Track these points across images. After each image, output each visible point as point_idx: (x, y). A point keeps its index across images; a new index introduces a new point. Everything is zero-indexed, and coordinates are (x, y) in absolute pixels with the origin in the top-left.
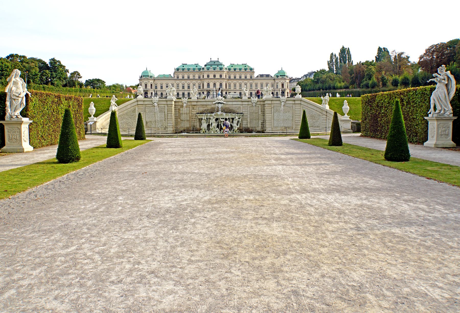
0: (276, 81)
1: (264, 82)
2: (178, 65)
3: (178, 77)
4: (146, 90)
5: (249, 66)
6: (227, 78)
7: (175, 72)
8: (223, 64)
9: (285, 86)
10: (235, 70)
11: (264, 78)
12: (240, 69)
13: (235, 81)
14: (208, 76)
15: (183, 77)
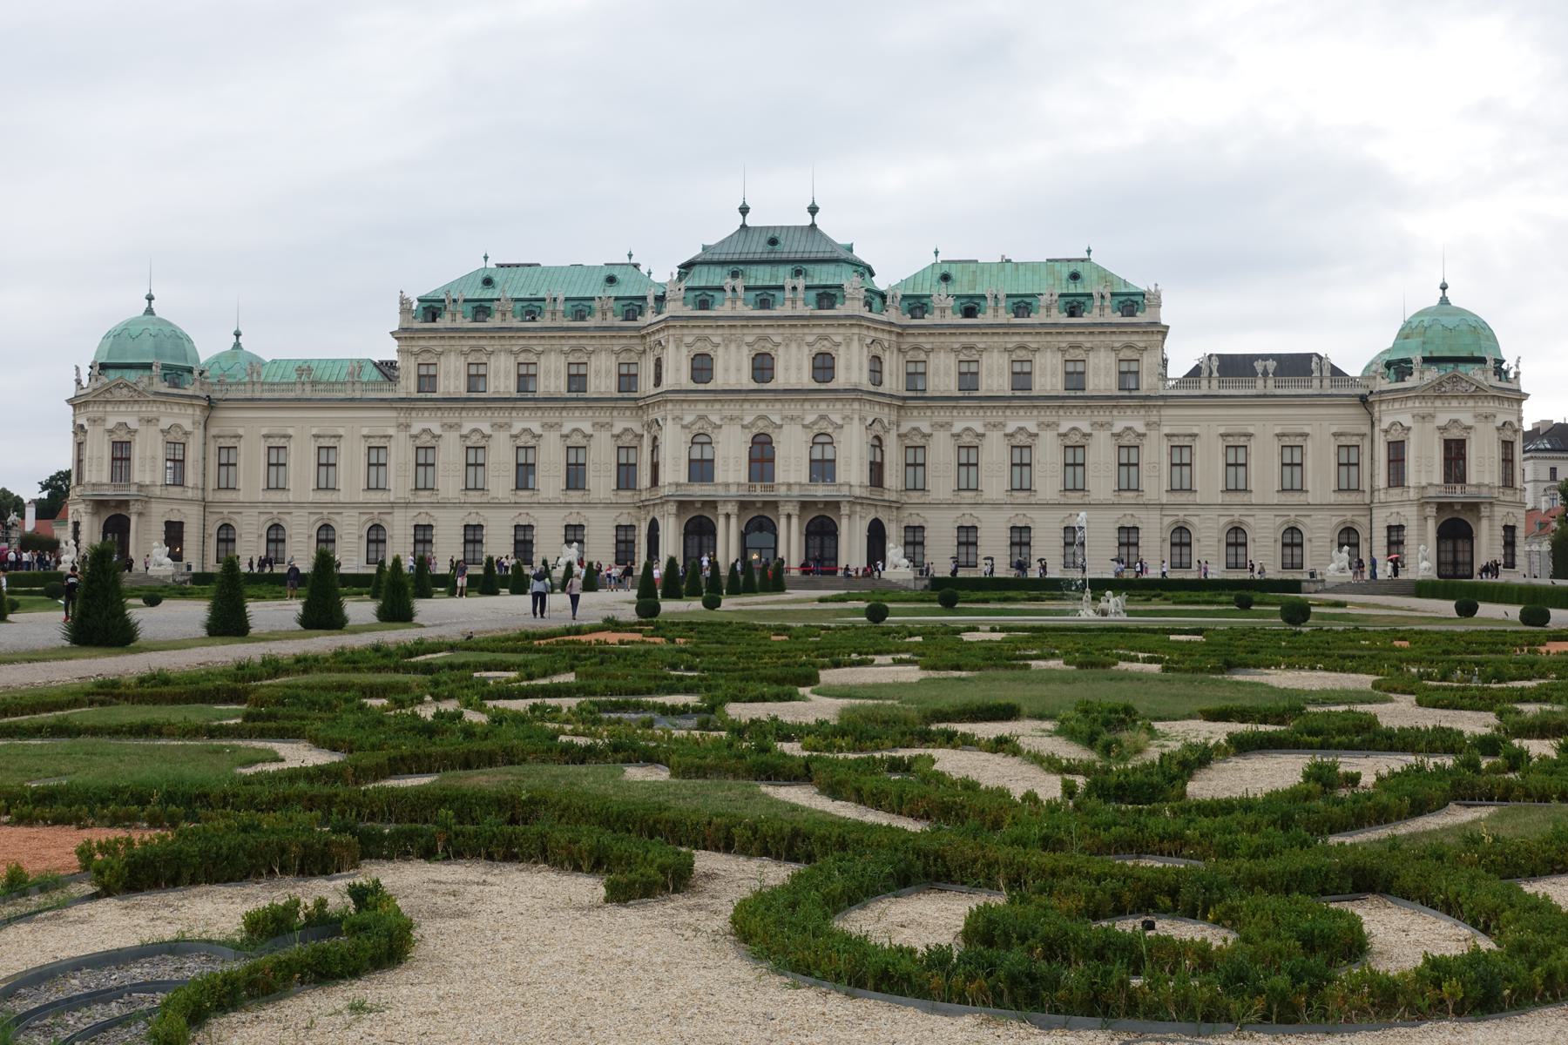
0: (1388, 416)
1: (1266, 429)
2: (442, 268)
3: (427, 381)
4: (109, 493)
5: (1106, 277)
6: (893, 382)
7: (403, 334)
8: (860, 253)
9: (1482, 468)
10: (969, 312)
11: (1259, 387)
12: (1022, 305)
13: (968, 421)
14: (702, 367)
15: (475, 380)
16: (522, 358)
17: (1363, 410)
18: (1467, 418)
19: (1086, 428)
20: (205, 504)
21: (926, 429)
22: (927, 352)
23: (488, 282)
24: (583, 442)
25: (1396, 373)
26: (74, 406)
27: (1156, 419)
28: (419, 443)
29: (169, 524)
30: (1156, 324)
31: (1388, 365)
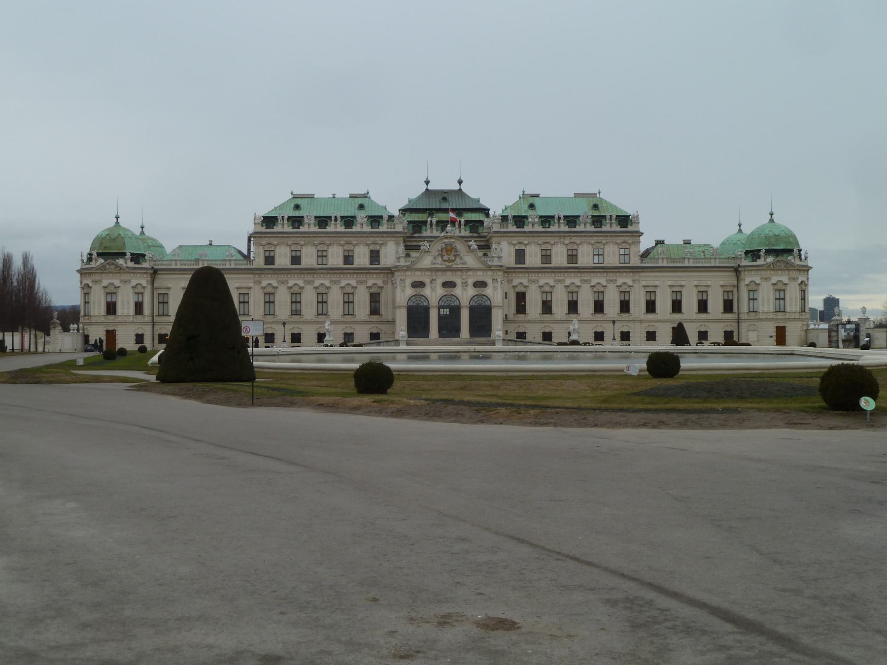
0: (748, 278)
3: (270, 260)
12: (572, 221)
15: (296, 260)
16: (319, 248)
17: (733, 274)
18: (785, 280)
19: (604, 283)
20: (153, 323)
21: (526, 283)
22: (526, 245)
23: (297, 207)
24: (352, 291)
25: (753, 256)
26: (81, 274)
27: (637, 278)
28: (266, 291)
29: (137, 335)
30: (637, 232)
31: (747, 253)
